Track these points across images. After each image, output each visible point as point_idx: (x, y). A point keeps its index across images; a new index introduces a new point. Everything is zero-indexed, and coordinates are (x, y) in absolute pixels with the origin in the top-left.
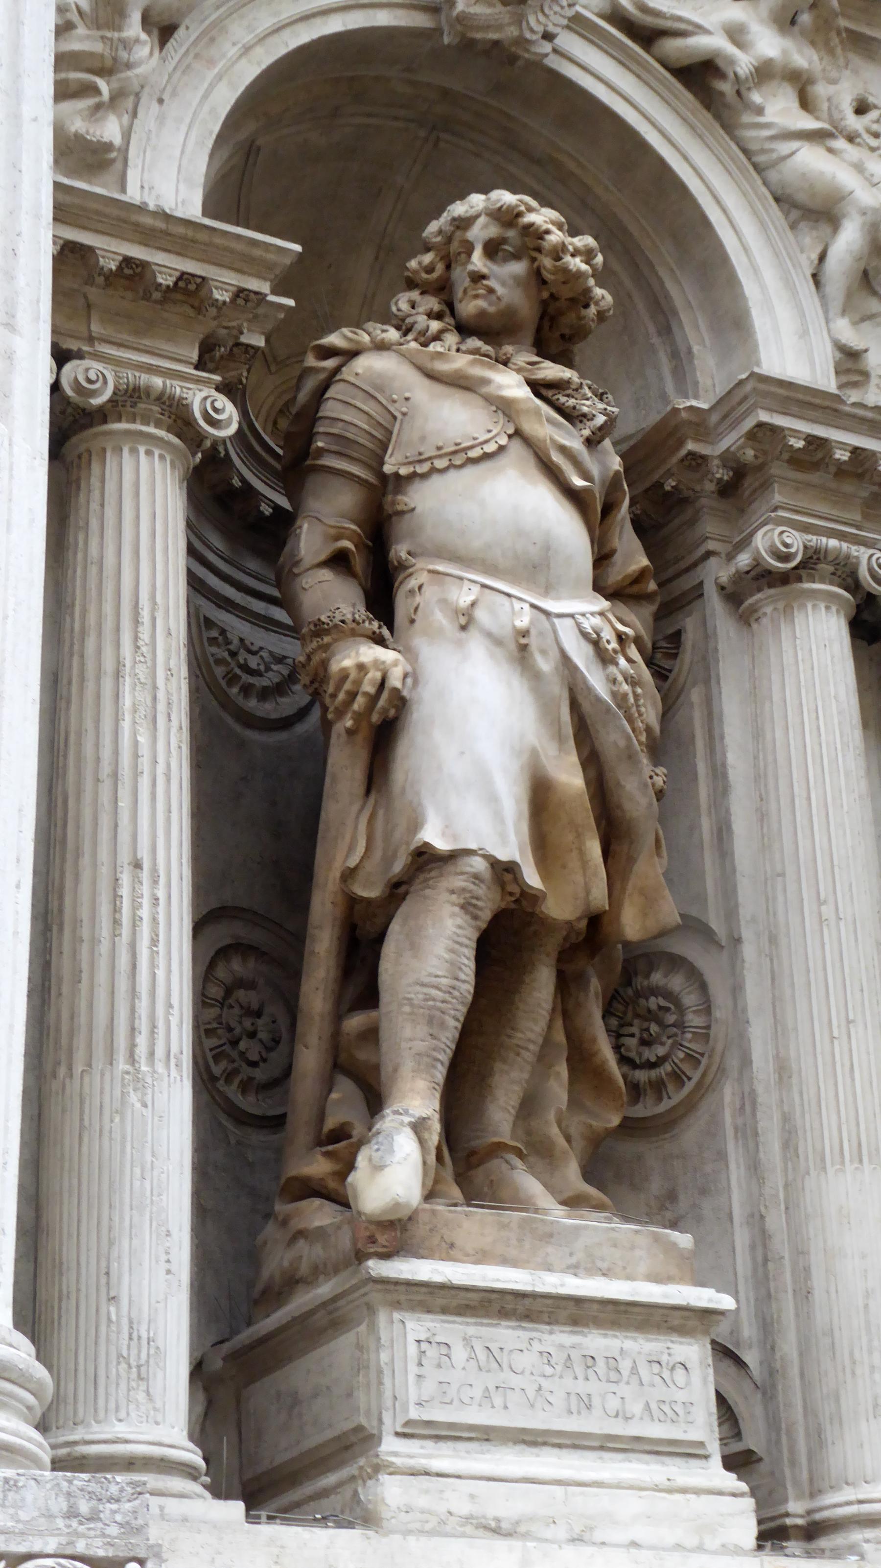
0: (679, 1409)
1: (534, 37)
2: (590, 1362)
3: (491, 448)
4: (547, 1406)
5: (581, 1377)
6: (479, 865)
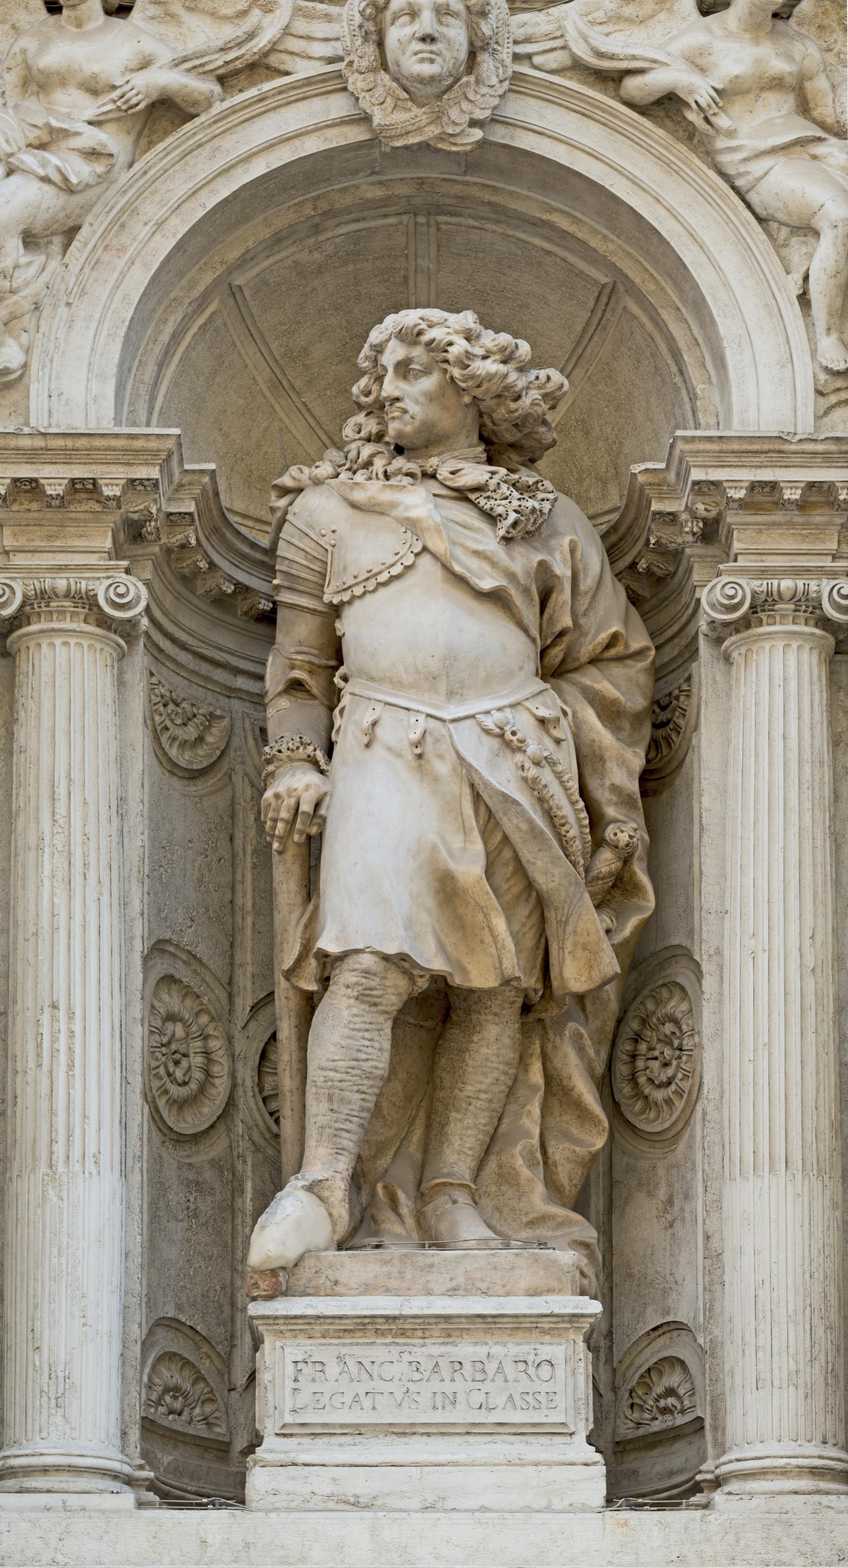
0: (542, 1398)
1: (458, 130)
2: (457, 1366)
3: (397, 570)
4: (414, 1406)
5: (447, 1380)
6: (367, 961)
